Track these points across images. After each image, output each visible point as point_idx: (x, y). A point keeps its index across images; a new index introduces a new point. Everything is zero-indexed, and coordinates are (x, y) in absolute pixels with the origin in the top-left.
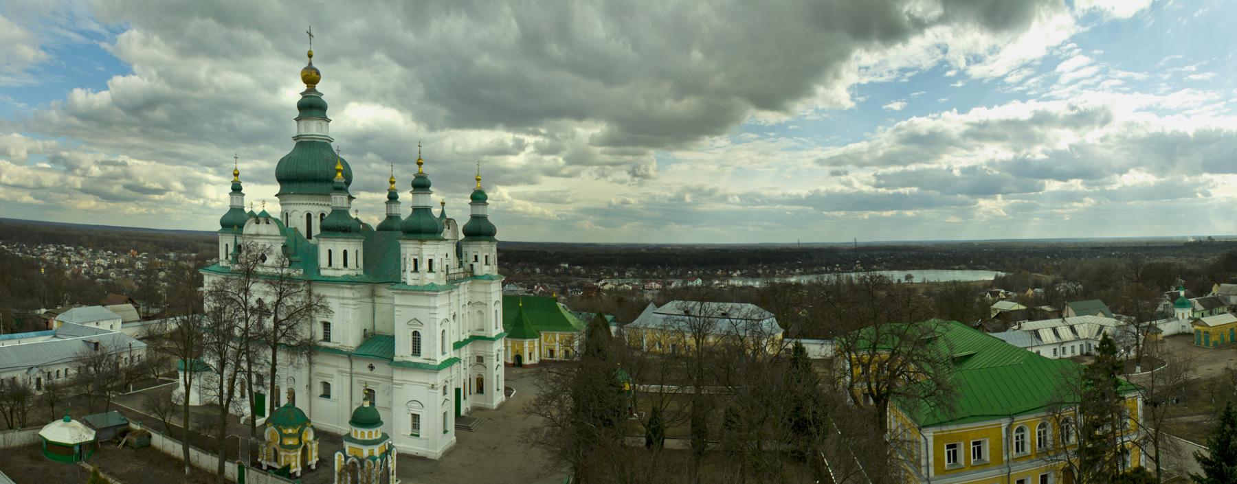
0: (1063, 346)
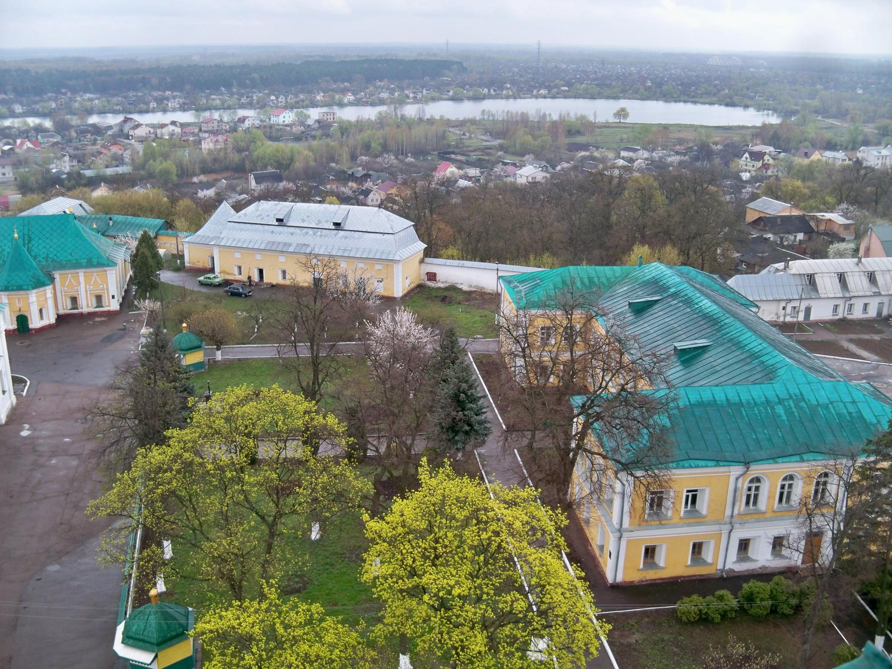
0: (852, 302)
